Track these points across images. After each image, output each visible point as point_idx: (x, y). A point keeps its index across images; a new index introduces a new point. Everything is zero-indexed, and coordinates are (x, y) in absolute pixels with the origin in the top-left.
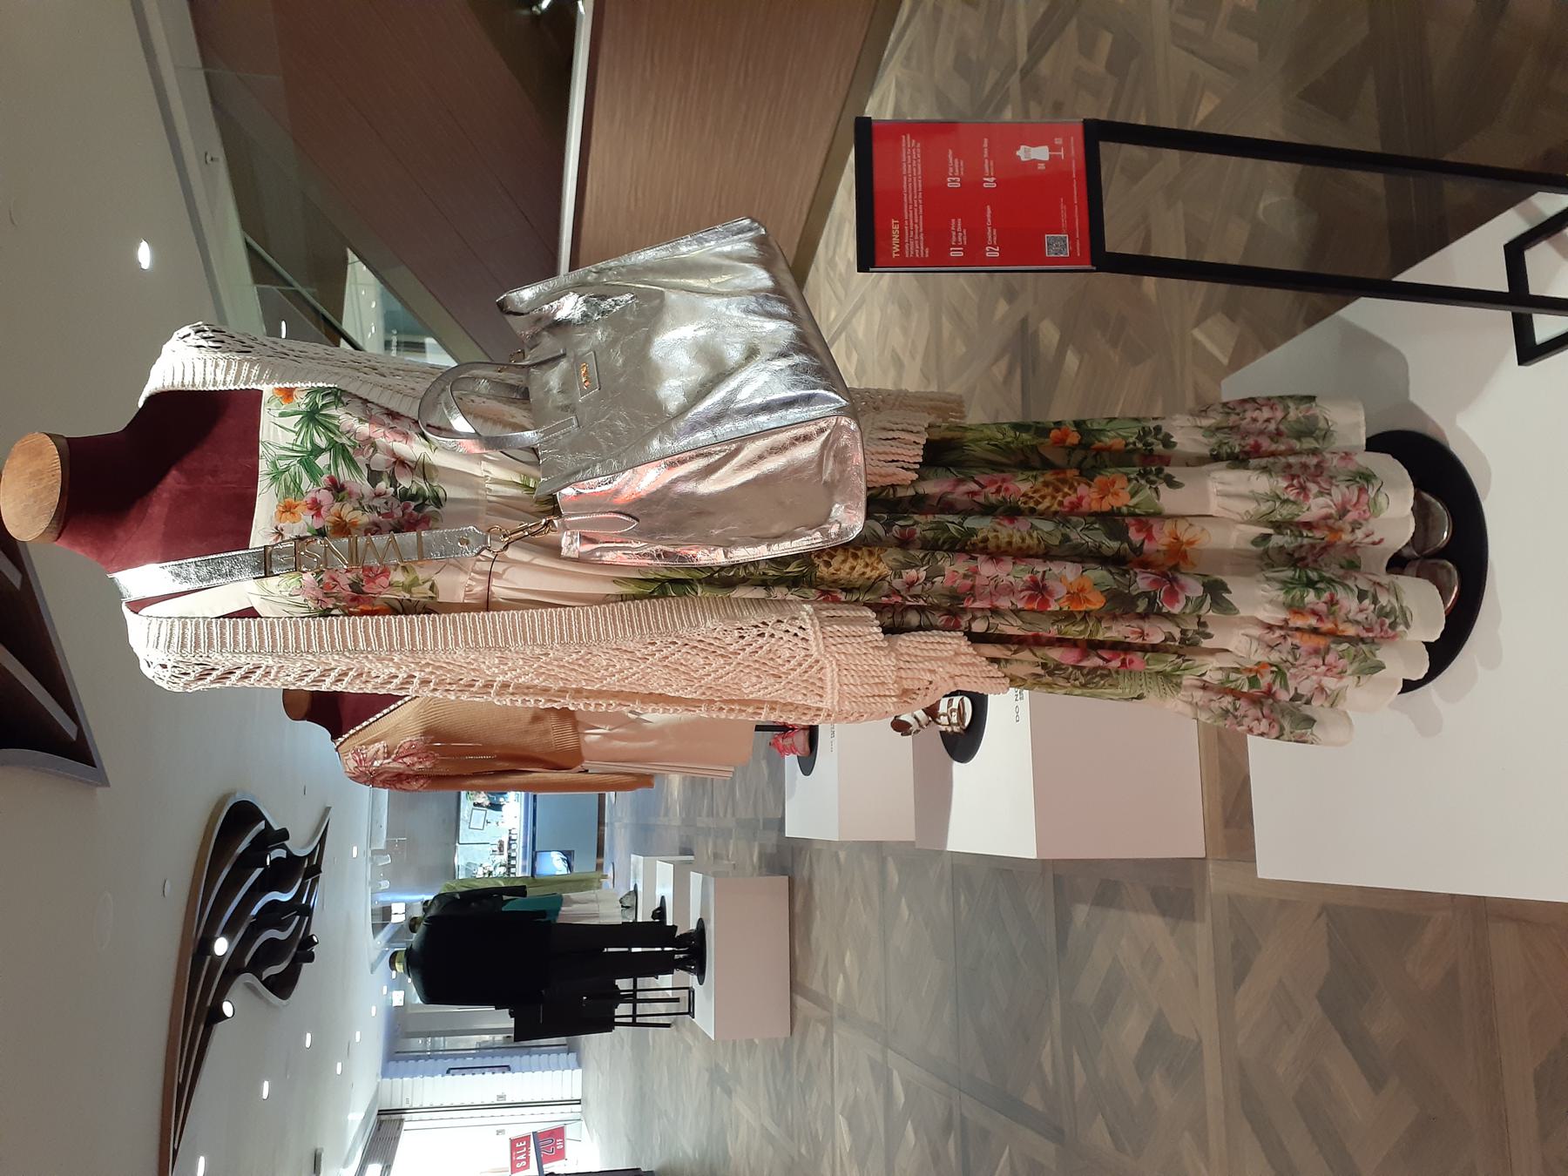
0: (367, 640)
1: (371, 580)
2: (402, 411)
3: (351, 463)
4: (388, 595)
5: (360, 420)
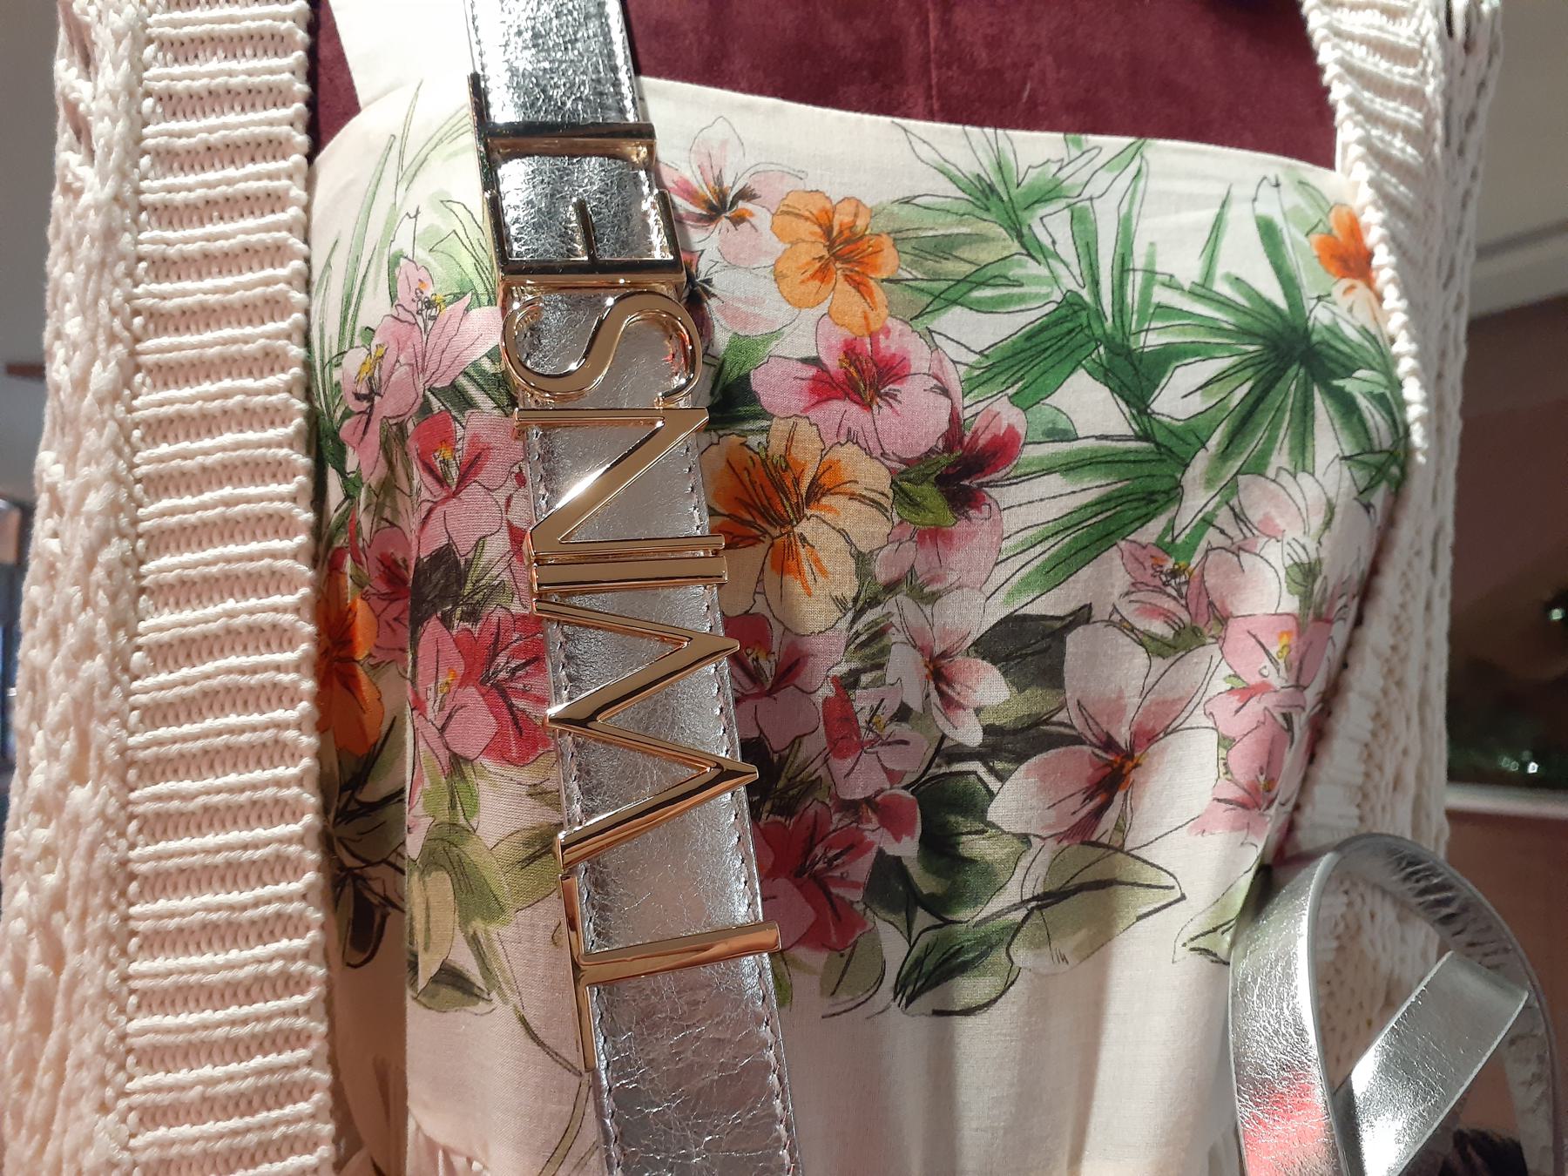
1: (477, 663)
3: (1090, 536)
4: (415, 766)
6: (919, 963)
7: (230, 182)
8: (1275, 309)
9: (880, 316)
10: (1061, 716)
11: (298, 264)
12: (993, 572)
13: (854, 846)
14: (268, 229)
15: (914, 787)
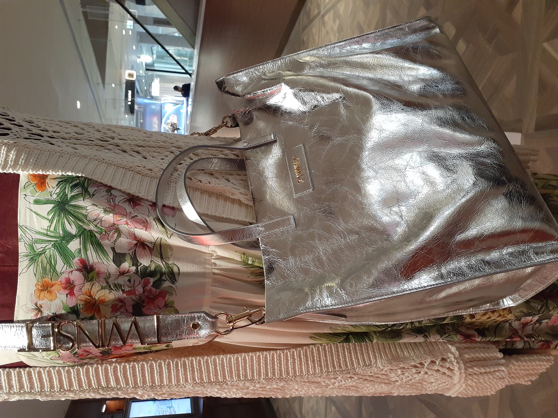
0: (117, 381)
2: (141, 194)
3: (98, 246)
5: (105, 211)
6: (170, 279)
7: (36, 379)
8: (53, 208)
9: (58, 282)
10: (131, 254)
11: (51, 369)
12: (105, 263)
13: (150, 291)
14: (45, 373)
15: (142, 278)
